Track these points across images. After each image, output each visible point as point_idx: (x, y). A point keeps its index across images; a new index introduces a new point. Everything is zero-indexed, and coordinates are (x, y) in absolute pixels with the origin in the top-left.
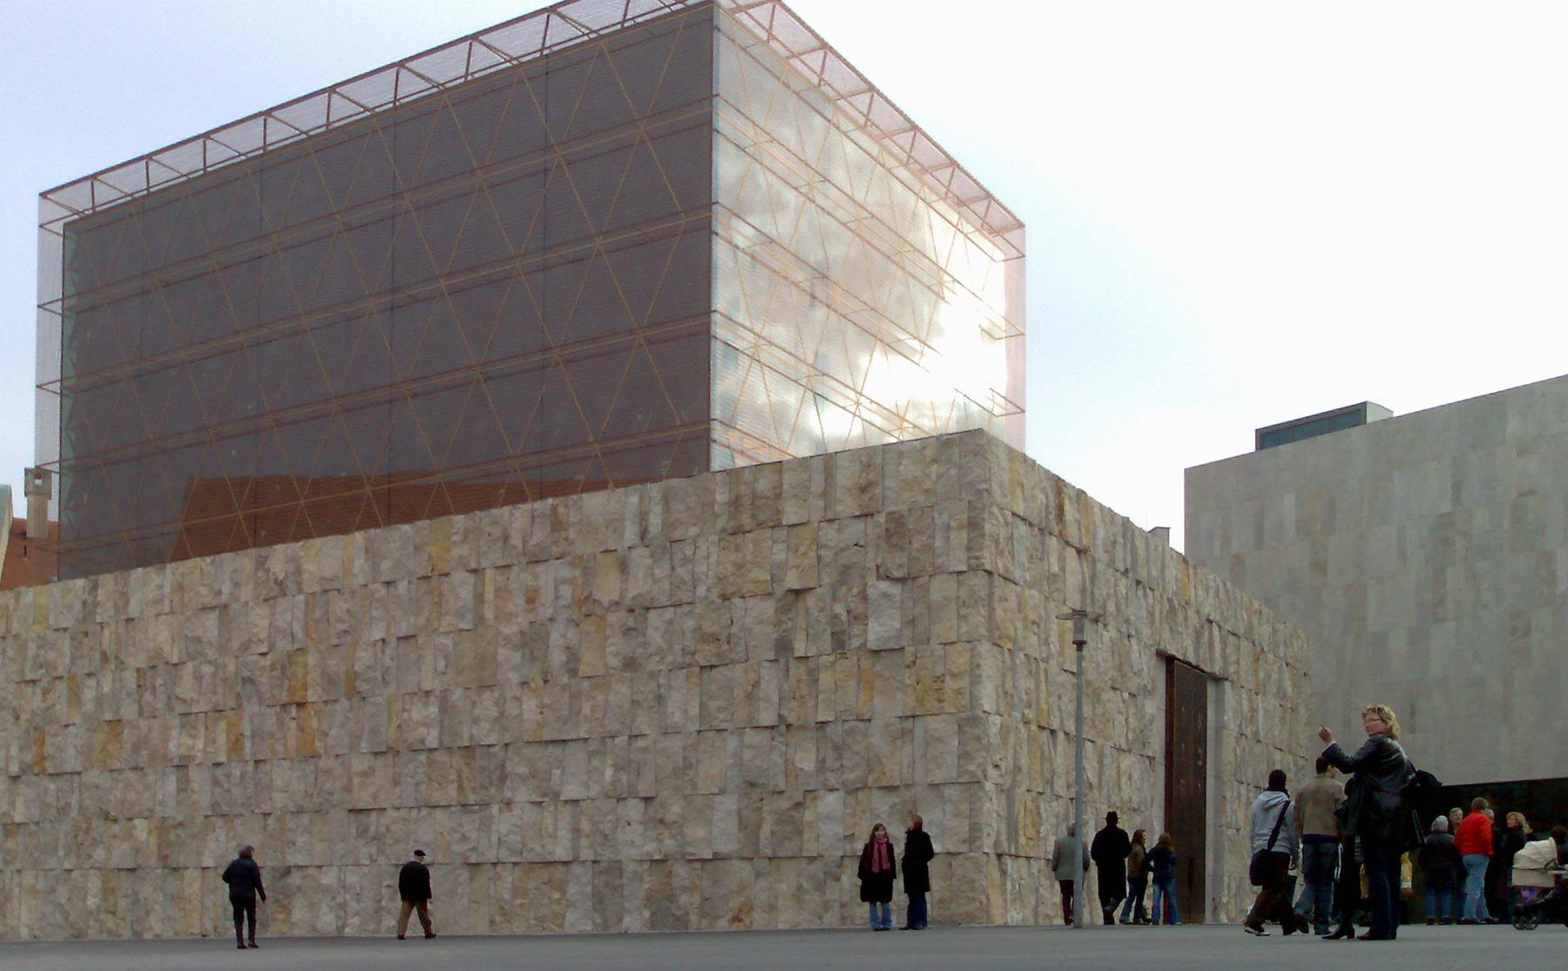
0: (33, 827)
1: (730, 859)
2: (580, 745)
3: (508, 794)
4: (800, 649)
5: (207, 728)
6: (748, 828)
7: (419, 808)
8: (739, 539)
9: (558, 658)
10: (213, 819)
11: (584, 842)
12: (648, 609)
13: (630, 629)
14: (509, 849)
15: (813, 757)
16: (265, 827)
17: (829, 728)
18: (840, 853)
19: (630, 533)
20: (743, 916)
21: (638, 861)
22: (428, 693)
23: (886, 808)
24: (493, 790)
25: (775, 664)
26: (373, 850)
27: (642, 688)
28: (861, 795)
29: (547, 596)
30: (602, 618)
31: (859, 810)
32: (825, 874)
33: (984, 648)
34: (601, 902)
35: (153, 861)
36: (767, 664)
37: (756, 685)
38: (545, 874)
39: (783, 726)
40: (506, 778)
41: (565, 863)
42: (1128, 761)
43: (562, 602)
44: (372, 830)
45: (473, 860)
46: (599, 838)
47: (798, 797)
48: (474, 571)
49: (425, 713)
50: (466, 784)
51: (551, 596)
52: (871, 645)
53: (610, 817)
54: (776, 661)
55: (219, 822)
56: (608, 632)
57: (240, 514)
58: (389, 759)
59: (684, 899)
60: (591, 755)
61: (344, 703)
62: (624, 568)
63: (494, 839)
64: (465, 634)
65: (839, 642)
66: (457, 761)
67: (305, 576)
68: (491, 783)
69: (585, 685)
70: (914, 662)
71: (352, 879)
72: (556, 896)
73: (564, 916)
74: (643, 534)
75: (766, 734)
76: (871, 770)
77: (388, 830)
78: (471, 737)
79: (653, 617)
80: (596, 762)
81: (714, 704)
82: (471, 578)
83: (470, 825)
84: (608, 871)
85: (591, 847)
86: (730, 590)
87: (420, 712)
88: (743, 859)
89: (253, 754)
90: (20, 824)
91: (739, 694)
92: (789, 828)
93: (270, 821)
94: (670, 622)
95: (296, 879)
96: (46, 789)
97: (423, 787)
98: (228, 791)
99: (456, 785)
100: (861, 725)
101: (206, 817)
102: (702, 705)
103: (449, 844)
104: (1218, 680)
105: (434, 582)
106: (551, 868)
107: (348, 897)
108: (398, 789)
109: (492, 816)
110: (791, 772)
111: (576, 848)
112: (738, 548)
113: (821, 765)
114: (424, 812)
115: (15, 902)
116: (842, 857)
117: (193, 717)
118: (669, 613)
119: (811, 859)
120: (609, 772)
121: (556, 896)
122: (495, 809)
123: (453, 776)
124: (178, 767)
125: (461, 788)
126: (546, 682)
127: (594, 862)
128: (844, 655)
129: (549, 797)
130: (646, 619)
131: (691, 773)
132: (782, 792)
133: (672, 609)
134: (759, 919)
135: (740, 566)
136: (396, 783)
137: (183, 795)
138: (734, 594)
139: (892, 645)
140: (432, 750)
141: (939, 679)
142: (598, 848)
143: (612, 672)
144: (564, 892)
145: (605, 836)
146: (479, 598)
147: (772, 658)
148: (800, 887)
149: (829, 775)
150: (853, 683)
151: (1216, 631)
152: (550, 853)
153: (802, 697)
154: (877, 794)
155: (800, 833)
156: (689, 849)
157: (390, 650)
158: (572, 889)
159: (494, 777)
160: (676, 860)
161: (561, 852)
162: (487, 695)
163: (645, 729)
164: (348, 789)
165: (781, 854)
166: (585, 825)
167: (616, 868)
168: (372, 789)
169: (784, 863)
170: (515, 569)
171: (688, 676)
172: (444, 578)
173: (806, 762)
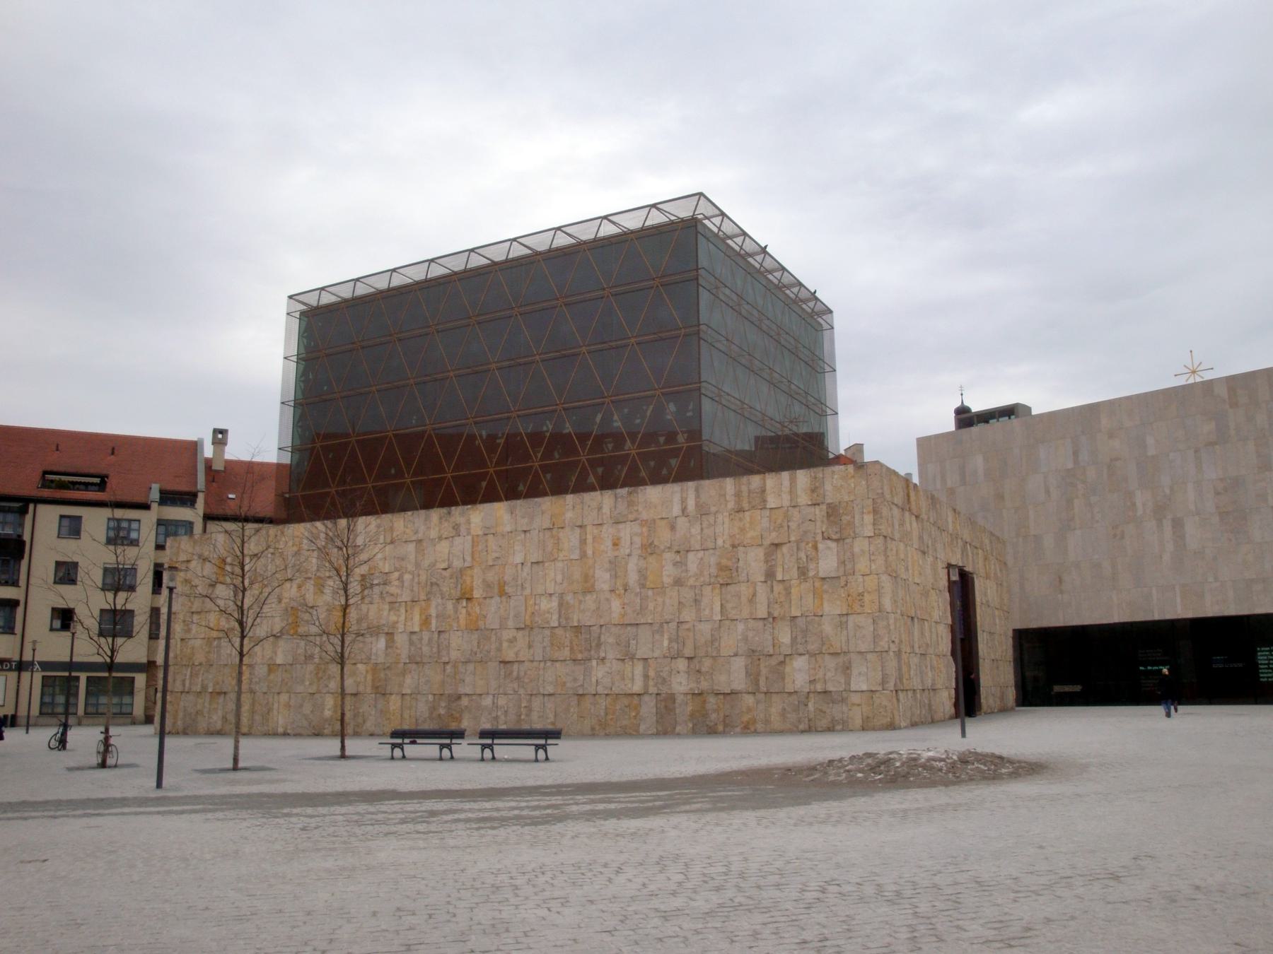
1: (741, 693)
3: (602, 655)
4: (779, 577)
5: (406, 611)
6: (753, 675)
7: (545, 661)
8: (741, 515)
9: (633, 578)
10: (410, 665)
11: (651, 683)
12: (687, 551)
13: (677, 562)
14: (604, 687)
15: (789, 636)
16: (444, 671)
18: (808, 690)
21: (684, 694)
22: (551, 595)
24: (593, 652)
25: (765, 584)
26: (516, 685)
27: (685, 595)
28: (819, 658)
29: (625, 542)
31: (817, 666)
32: (799, 702)
33: (884, 578)
35: (369, 690)
36: (760, 584)
37: (754, 595)
38: (626, 701)
39: (772, 619)
40: (601, 644)
41: (639, 695)
44: (515, 674)
45: (580, 692)
47: (781, 658)
49: (549, 606)
50: (575, 648)
51: (628, 543)
52: (822, 575)
53: (667, 668)
54: (765, 582)
55: (414, 666)
56: (664, 562)
57: (408, 481)
58: (526, 632)
59: (714, 716)
61: (497, 599)
62: (673, 528)
63: (594, 680)
64: (574, 561)
65: (803, 572)
67: (472, 525)
68: (591, 647)
69: (650, 593)
70: (846, 585)
71: (502, 701)
74: (684, 510)
75: (761, 623)
76: (823, 644)
77: (525, 674)
78: (579, 621)
79: (691, 556)
81: (729, 606)
82: (578, 531)
85: (656, 685)
86: (737, 542)
87: (545, 604)
88: (749, 693)
89: (437, 628)
90: (279, 665)
91: (744, 599)
93: (448, 668)
94: (702, 559)
95: (465, 701)
97: (548, 649)
98: (421, 649)
99: (569, 648)
100: (816, 618)
101: (405, 663)
102: (722, 605)
103: (565, 683)
105: (554, 532)
107: (499, 713)
108: (531, 651)
109: (592, 666)
111: (646, 686)
112: (741, 520)
113: (794, 640)
114: (549, 664)
115: (275, 712)
116: (808, 693)
117: (398, 604)
118: (701, 554)
119: (790, 694)
120: (666, 643)
122: (594, 663)
123: (567, 643)
124: (387, 633)
125: (572, 649)
126: (626, 590)
127: (657, 694)
128: (805, 580)
129: (628, 656)
130: (687, 557)
132: (771, 655)
133: (702, 552)
135: (742, 530)
136: (530, 647)
137: (389, 650)
138: (739, 545)
139: (833, 575)
140: (554, 628)
141: (861, 595)
142: (660, 686)
143: (666, 585)
145: (664, 679)
146: (583, 542)
147: (763, 580)
148: (784, 709)
149: (799, 646)
152: (630, 689)
153: (781, 602)
154: (827, 657)
155: (783, 679)
156: (716, 688)
157: (527, 569)
160: (708, 693)
161: (637, 687)
162: (588, 597)
163: (687, 618)
164: (499, 649)
165: (771, 691)
166: (652, 673)
167: (672, 698)
168: (516, 649)
169: (774, 696)
172: (560, 530)
173: (785, 638)
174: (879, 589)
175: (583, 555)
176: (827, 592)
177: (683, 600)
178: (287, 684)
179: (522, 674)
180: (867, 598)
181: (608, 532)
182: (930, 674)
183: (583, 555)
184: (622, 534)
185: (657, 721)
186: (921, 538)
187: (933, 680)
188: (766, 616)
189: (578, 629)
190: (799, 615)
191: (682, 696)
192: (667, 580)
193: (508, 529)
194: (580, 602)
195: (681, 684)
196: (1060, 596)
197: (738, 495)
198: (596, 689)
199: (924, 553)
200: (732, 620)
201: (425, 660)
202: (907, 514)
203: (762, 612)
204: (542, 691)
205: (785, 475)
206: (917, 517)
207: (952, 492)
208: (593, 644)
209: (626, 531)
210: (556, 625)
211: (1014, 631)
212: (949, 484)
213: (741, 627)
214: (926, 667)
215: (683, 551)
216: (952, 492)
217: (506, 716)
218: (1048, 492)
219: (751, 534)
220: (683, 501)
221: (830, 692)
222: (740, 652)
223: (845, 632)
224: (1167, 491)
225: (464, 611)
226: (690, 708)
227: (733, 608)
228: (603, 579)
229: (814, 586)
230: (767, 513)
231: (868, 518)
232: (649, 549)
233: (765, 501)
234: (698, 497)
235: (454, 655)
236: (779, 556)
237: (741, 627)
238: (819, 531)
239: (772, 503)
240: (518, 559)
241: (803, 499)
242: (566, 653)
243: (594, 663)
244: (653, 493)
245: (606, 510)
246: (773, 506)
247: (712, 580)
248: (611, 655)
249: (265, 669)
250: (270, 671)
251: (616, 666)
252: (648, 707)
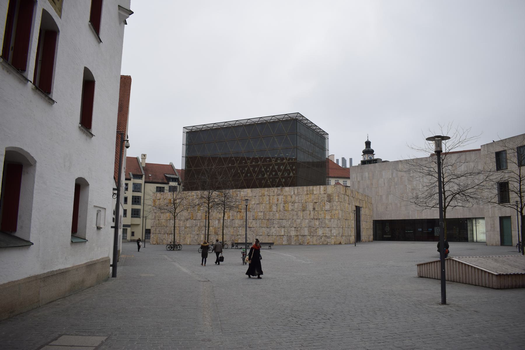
0: (190, 228)
2: (285, 220)
6: (310, 232)
7: (260, 227)
8: (308, 195)
15: (318, 223)
17: (320, 220)
19: (292, 193)
23: (328, 230)
24: (272, 225)
26: (252, 233)
29: (280, 200)
30: (288, 203)
34: (288, 241)
35: (213, 233)
38: (280, 237)
43: (282, 201)
45: (269, 235)
46: (288, 232)
48: (269, 196)
49: (261, 214)
52: (326, 210)
54: (313, 211)
58: (255, 220)
59: (300, 241)
60: (287, 221)
62: (291, 197)
63: (272, 232)
66: (266, 221)
69: (286, 212)
72: (281, 240)
73: (283, 243)
77: (255, 230)
78: (268, 218)
79: (296, 204)
80: (287, 222)
81: (304, 216)
82: (268, 197)
83: (268, 230)
84: (289, 237)
87: (260, 214)
91: (308, 215)
92: (315, 232)
94: (298, 205)
96: (193, 222)
103: (265, 233)
104: (361, 207)
106: (281, 236)
108: (256, 225)
110: (315, 224)
111: (285, 234)
112: (307, 196)
113: (319, 224)
114: (261, 228)
115: (187, 239)
118: (298, 204)
121: (281, 240)
122: (272, 228)
123: (266, 223)
129: (281, 227)
131: (301, 224)
134: (311, 243)
136: (256, 224)
140: (262, 219)
144: (283, 240)
146: (270, 199)
148: (317, 239)
150: (323, 214)
155: (317, 233)
158: (284, 239)
159: (272, 224)
161: (283, 233)
165: (314, 235)
166: (286, 231)
167: (291, 236)
170: (275, 196)
171: (301, 212)
174: (339, 213)
175: (270, 203)
176: (327, 213)
177: (294, 214)
178: (190, 232)
179: (254, 230)
180: (336, 215)
181: (276, 197)
182: (350, 232)
183: (270, 203)
184: (279, 198)
185: (287, 242)
186: (348, 201)
187: (350, 234)
189: (268, 220)
191: (293, 236)
192: (290, 209)
193: (251, 195)
194: (269, 214)
195: (293, 233)
196: (386, 212)
197: (307, 191)
199: (349, 204)
200: (305, 219)
201: (228, 226)
202: (345, 196)
203: (312, 217)
204: (259, 234)
205: (318, 187)
206: (348, 196)
207: (359, 182)
208: (272, 224)
209: (280, 197)
210: (263, 219)
211: (373, 220)
212: (358, 180)
213: (307, 221)
214: (349, 231)
215: (294, 203)
216: (359, 182)
217: (250, 240)
218: (384, 184)
219: (310, 199)
220: (294, 191)
224: (415, 186)
225: (239, 215)
226: (295, 239)
227: (305, 216)
228: (274, 208)
230: (314, 195)
231: (337, 198)
232: (285, 202)
233: (313, 192)
234: (297, 190)
235: (236, 225)
236: (316, 205)
237: (307, 221)
238: (325, 200)
239: (315, 192)
240: (253, 203)
241: (322, 192)
242: (265, 226)
243: (272, 228)
244: (287, 189)
245: (275, 192)
246: (315, 194)
247: (301, 210)
248: (276, 226)
249: (184, 228)
250: (185, 228)
251: (278, 229)
252: (285, 238)
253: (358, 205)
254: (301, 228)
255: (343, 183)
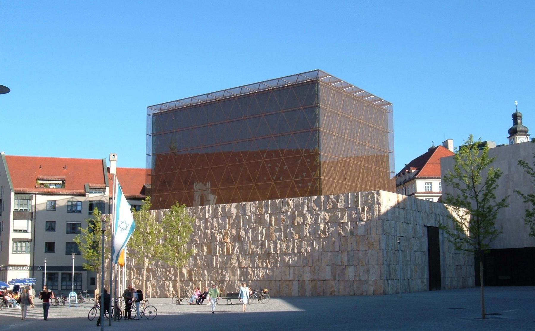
1: (329, 280)
20: (333, 293)
42: (417, 254)
47: (344, 267)
52: (359, 235)
70: (368, 239)
76: (359, 262)
100: (357, 252)
116: (354, 280)
127: (298, 281)
134: (336, 293)
141: (373, 243)
148: (345, 287)
150: (355, 242)
151: (441, 217)
161: (291, 278)
166: (296, 273)
167: (304, 282)
173: (345, 258)
180: (375, 244)
188: (339, 250)
190: (351, 250)
195: (307, 277)
198: (276, 279)
213: (329, 254)
221: (362, 280)
222: (329, 264)
223: (367, 257)
229: (356, 239)
253: (432, 223)
254: (320, 266)
255: (426, 187)
